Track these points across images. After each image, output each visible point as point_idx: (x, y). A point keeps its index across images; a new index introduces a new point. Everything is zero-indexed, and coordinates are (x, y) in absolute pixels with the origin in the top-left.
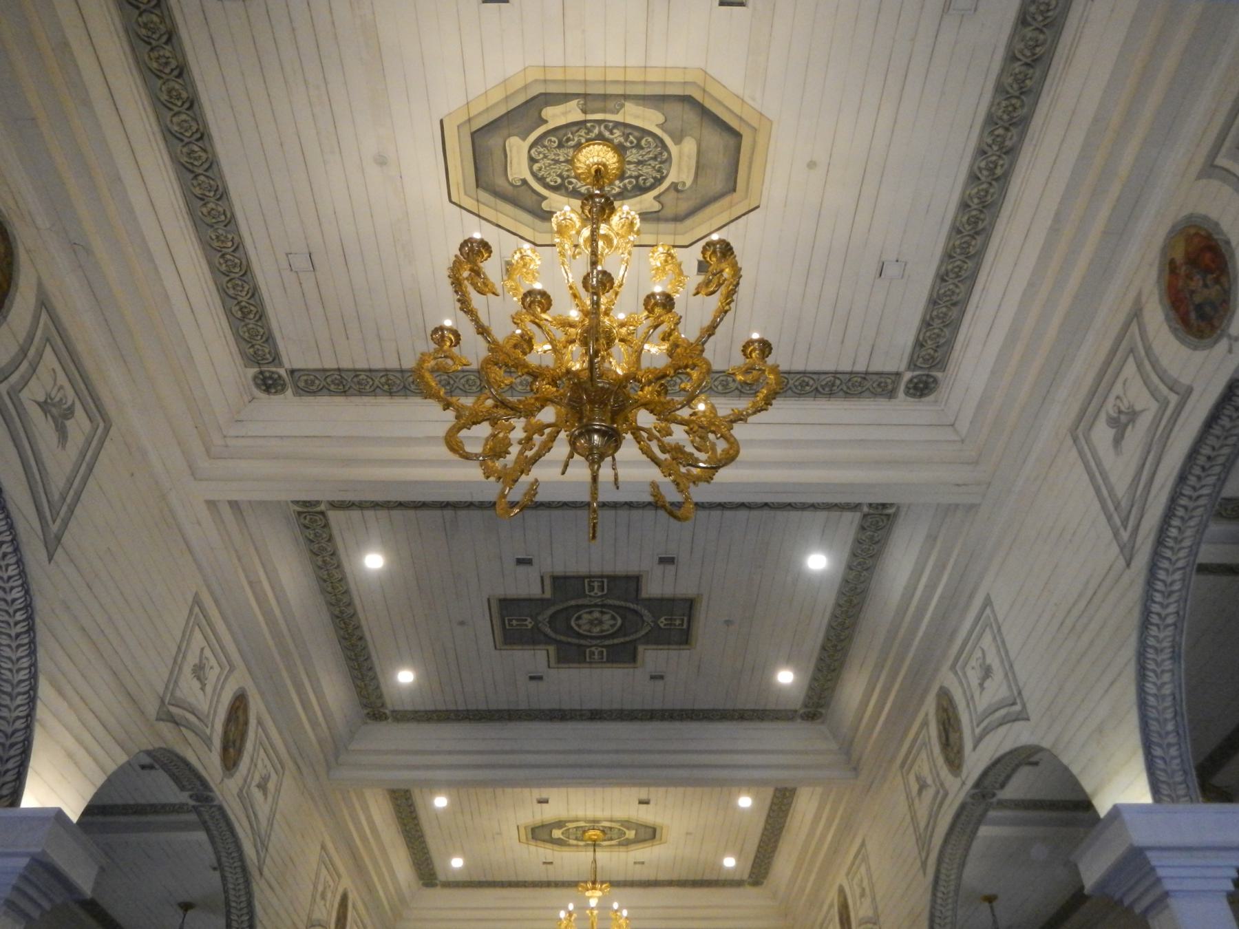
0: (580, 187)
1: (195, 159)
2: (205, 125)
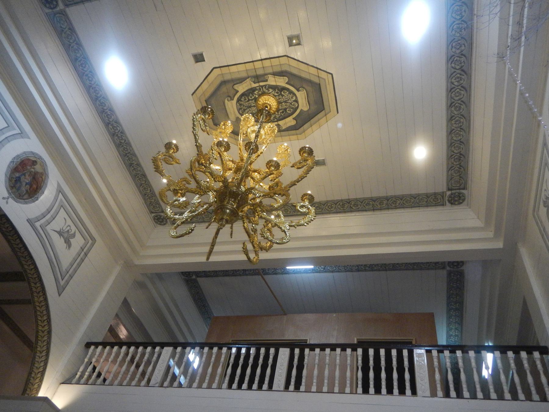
0: (273, 91)
1: (458, 77)
2: (447, 96)
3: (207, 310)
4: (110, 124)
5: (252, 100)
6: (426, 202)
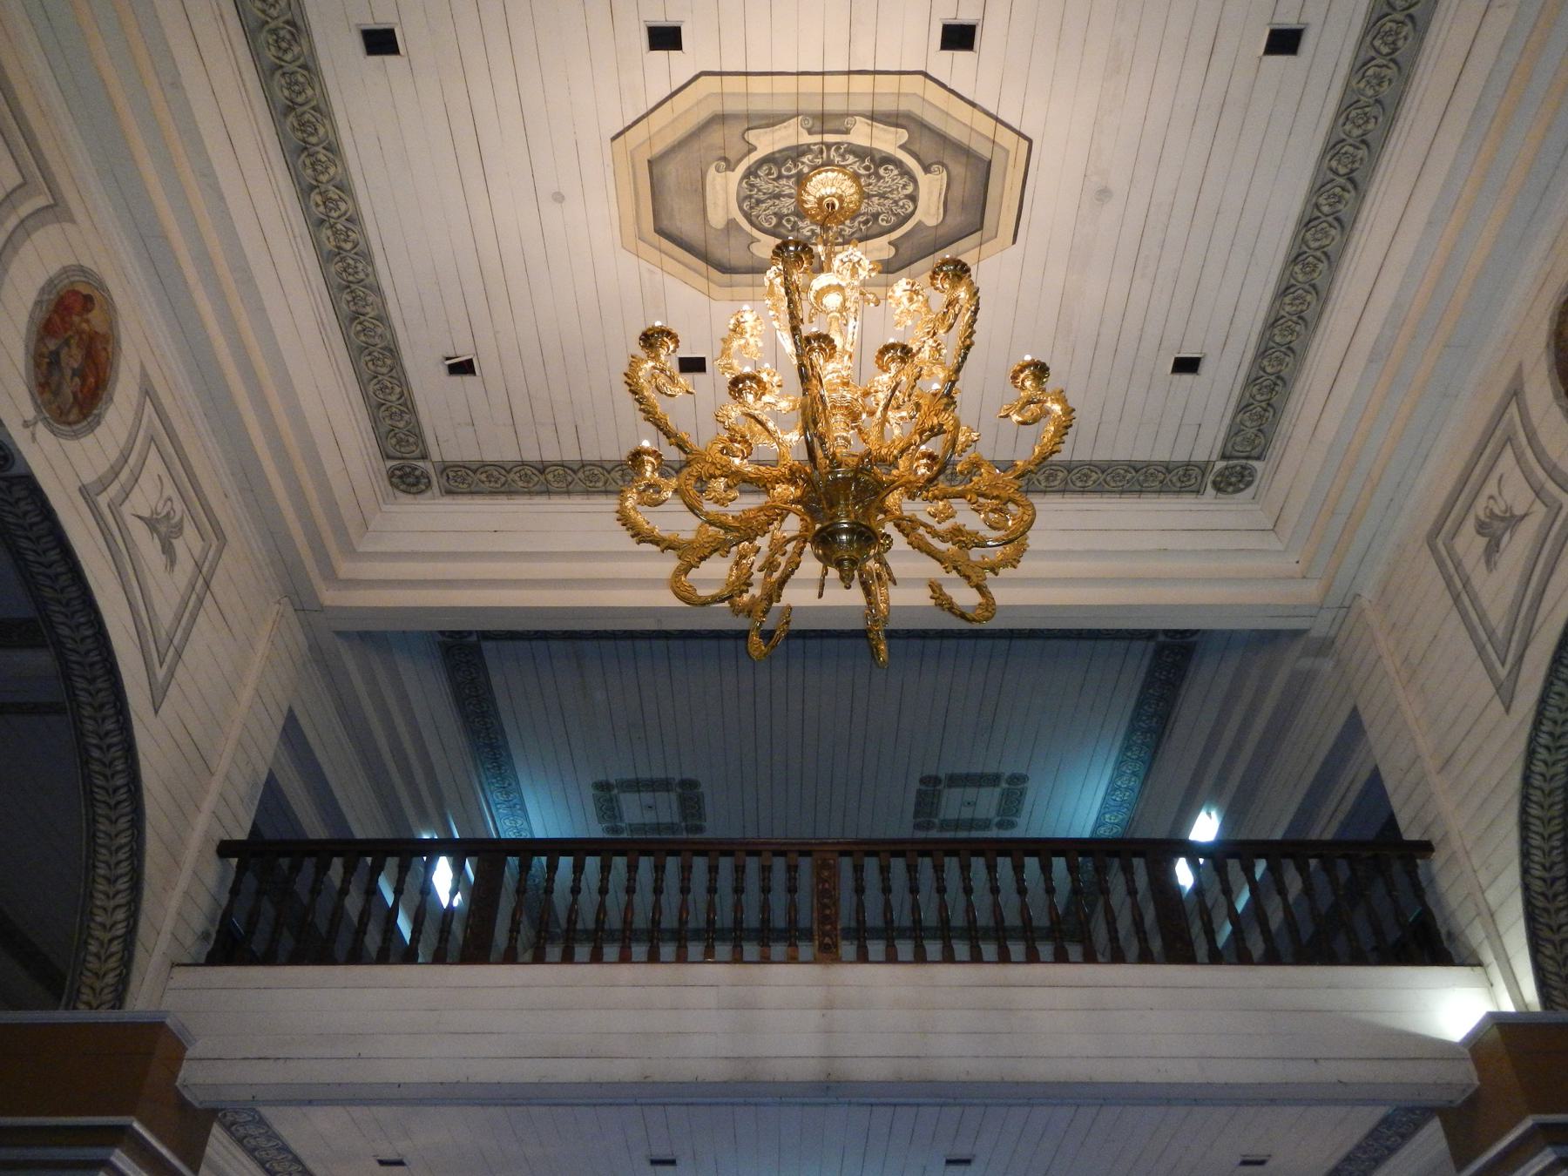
0: (855, 162)
1: (1335, 195)
3: (489, 725)
4: (317, 190)
5: (788, 178)
6: (1161, 482)
